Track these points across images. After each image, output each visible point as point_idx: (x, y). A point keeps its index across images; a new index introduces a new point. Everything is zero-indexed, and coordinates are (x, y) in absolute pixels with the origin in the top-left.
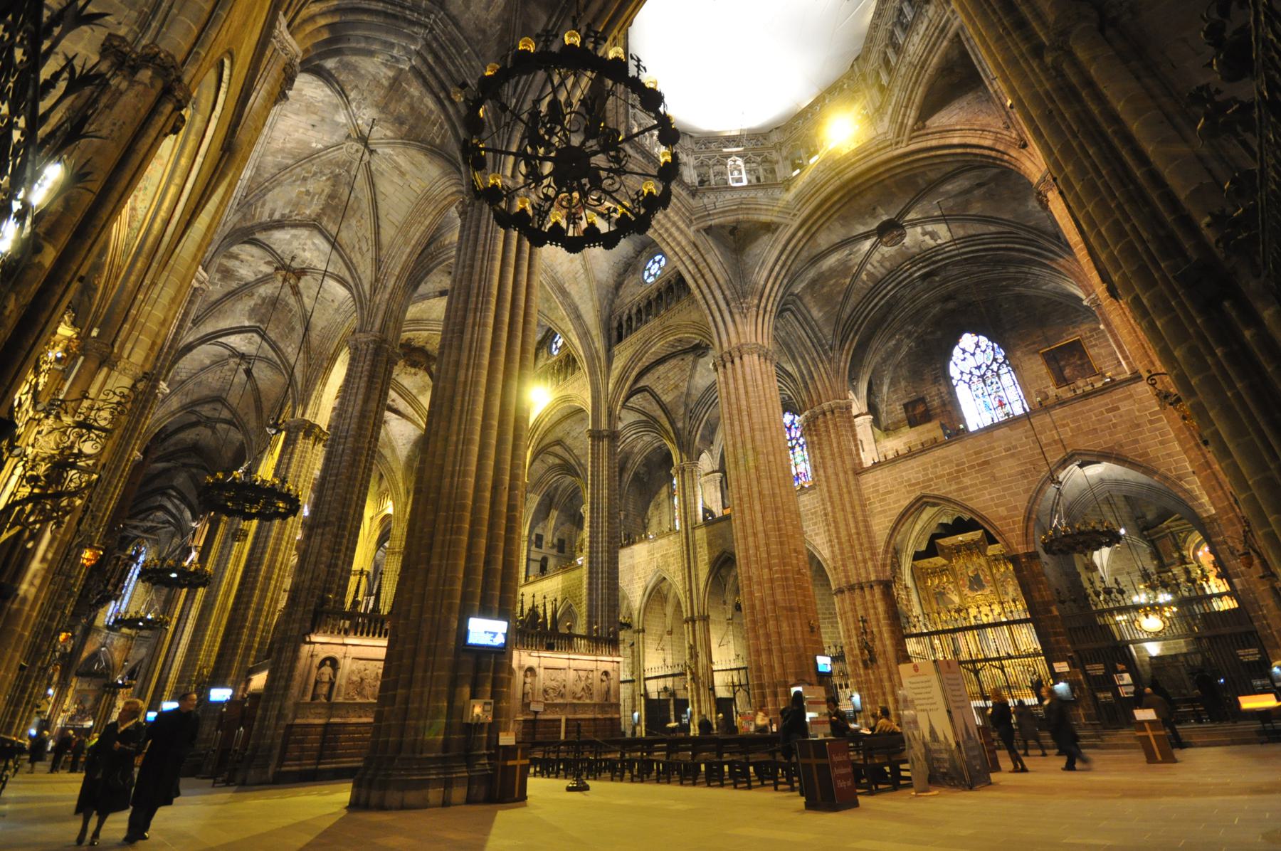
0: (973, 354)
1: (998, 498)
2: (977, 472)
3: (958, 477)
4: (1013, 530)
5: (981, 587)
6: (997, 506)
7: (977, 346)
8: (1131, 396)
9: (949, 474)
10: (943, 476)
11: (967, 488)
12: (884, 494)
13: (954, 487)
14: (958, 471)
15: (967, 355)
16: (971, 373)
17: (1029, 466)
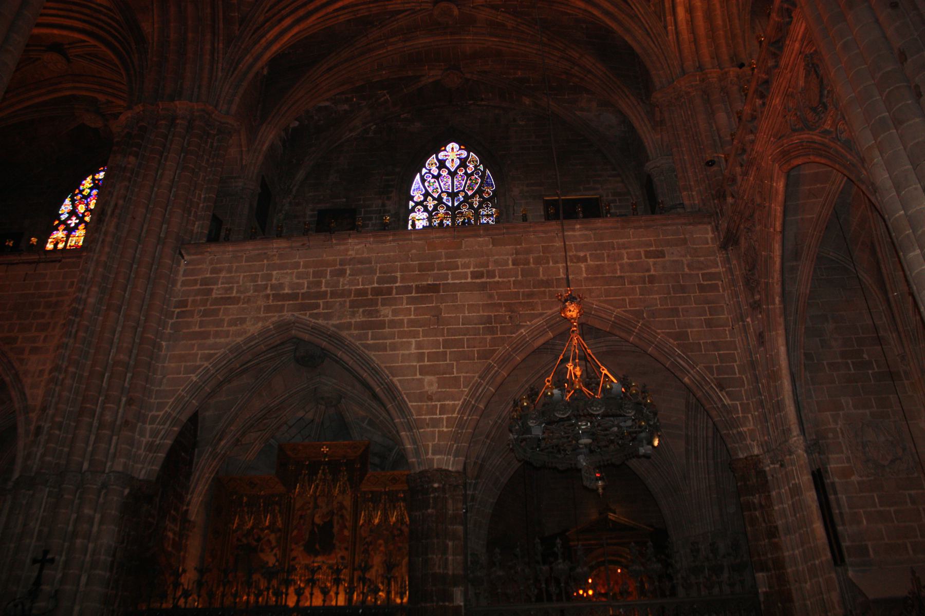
0: (453, 174)
1: (431, 357)
2: (412, 301)
3: (373, 303)
4: (436, 423)
5: (327, 548)
6: (424, 371)
7: (463, 163)
8: (684, 242)
9: (360, 293)
10: (344, 294)
11: (382, 325)
12: (217, 301)
13: (359, 318)
14: (377, 292)
15: (444, 173)
16: (440, 199)
17: (502, 311)
